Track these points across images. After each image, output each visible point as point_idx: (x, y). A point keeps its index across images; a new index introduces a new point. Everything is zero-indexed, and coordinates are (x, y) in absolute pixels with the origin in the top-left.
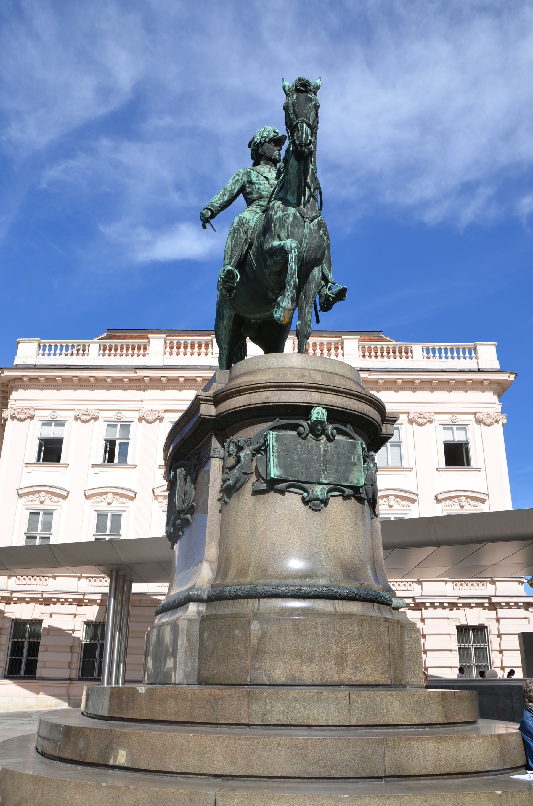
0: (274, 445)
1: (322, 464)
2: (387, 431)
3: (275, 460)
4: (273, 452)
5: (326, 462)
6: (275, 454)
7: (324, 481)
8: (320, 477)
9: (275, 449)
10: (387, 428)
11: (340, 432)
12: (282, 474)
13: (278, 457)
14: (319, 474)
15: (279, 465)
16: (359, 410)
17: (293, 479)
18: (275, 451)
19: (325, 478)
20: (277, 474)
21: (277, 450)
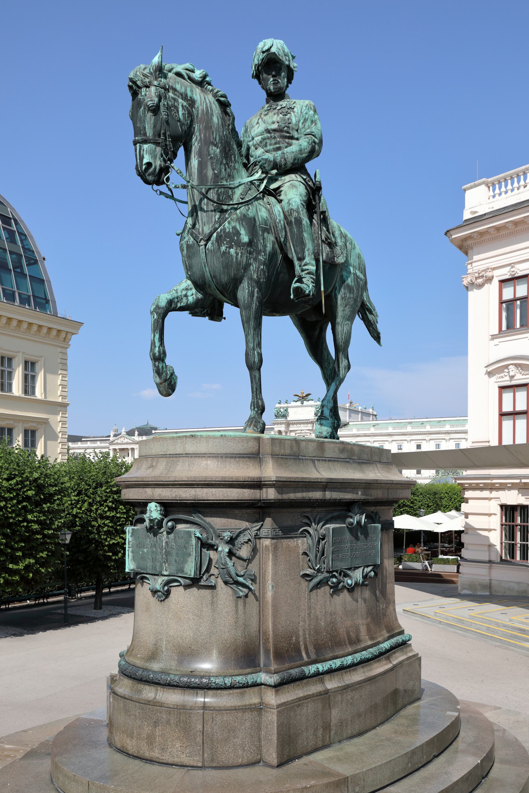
0: (130, 540)
1: (164, 556)
2: (267, 497)
3: (131, 554)
4: (129, 547)
5: (168, 554)
6: (130, 549)
7: (165, 573)
8: (162, 569)
9: (131, 543)
10: (267, 492)
11: (178, 521)
12: (135, 567)
13: (132, 552)
14: (161, 566)
15: (134, 559)
16: (191, 498)
17: (143, 571)
18: (130, 546)
19: (166, 571)
20: (132, 567)
21: (132, 545)
